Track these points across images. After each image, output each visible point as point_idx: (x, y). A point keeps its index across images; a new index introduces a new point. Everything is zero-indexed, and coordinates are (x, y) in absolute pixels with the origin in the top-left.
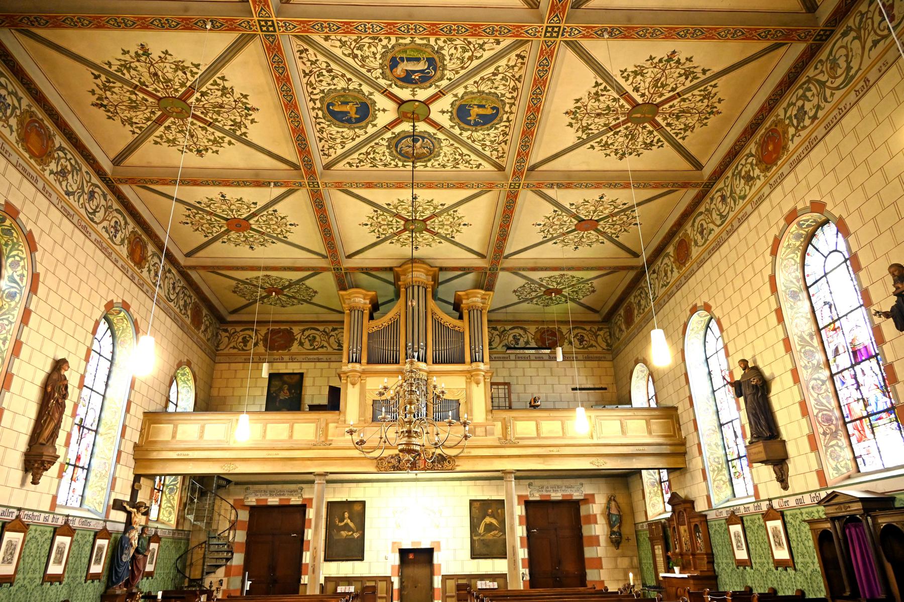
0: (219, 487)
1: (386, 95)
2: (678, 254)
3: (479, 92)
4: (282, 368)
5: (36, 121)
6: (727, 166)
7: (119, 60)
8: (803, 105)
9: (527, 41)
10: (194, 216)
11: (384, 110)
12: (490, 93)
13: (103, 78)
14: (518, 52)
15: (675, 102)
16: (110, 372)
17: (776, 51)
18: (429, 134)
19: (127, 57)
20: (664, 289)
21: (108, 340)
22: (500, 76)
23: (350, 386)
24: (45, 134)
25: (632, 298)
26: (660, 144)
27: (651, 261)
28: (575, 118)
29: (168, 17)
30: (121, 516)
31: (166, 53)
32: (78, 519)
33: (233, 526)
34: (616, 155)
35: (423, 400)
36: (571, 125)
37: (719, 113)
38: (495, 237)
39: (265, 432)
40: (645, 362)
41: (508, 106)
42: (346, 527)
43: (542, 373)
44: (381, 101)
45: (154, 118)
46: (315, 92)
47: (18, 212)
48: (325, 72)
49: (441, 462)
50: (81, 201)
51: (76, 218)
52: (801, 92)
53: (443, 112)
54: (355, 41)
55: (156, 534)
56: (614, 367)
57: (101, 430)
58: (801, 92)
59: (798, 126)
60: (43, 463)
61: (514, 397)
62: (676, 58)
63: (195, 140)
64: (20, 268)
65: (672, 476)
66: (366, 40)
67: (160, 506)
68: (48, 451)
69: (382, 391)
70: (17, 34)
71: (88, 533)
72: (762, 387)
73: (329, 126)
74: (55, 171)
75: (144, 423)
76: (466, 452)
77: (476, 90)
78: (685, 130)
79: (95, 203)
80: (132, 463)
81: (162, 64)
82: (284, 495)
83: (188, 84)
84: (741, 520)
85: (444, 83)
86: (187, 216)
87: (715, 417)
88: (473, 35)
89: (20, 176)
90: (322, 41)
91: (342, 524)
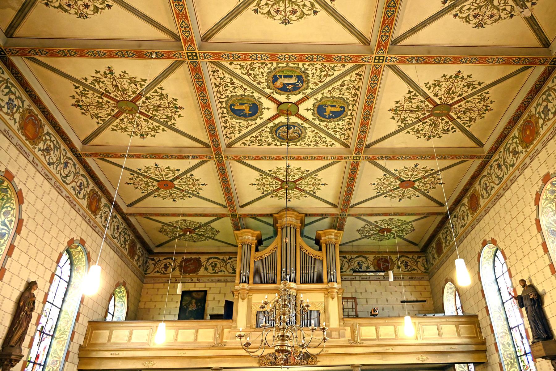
1: (270, 99)
2: (471, 204)
3: (331, 97)
4: (191, 287)
5: (33, 116)
6: (500, 144)
7: (93, 77)
8: (547, 105)
9: (363, 65)
10: (136, 179)
11: (268, 109)
12: (339, 97)
13: (81, 88)
14: (357, 72)
15: (462, 103)
16: (67, 291)
17: (525, 71)
18: (298, 124)
19: (98, 75)
20: (463, 229)
21: (68, 267)
22: (345, 87)
23: (240, 300)
24: (37, 124)
25: (441, 235)
26: (454, 130)
27: (452, 209)
28: (396, 114)
29: (127, 50)
31: (125, 72)
34: (424, 137)
36: (393, 118)
37: (491, 110)
38: (344, 193)
39: (177, 336)
40: (452, 281)
41: (351, 106)
43: (379, 289)
44: (266, 103)
45: (113, 114)
46: (222, 97)
47: (13, 177)
48: (229, 85)
50: (58, 169)
51: (53, 180)
52: (544, 97)
53: (307, 110)
54: (250, 65)
56: (430, 285)
57: (56, 335)
58: (544, 97)
59: (545, 118)
60: (11, 361)
61: (359, 308)
62: (461, 76)
63: (140, 128)
64: (10, 216)
66: (257, 64)
68: (15, 352)
69: (264, 305)
70: (26, 60)
72: (538, 300)
73: (231, 119)
74: (42, 148)
75: (88, 329)
76: (325, 351)
77: (329, 96)
78: (470, 121)
79: (68, 170)
80: (77, 361)
81: (121, 80)
83: (138, 92)
85: (308, 91)
86: (130, 179)
87: (505, 323)
88: (327, 61)
89: (18, 152)
90: (227, 65)
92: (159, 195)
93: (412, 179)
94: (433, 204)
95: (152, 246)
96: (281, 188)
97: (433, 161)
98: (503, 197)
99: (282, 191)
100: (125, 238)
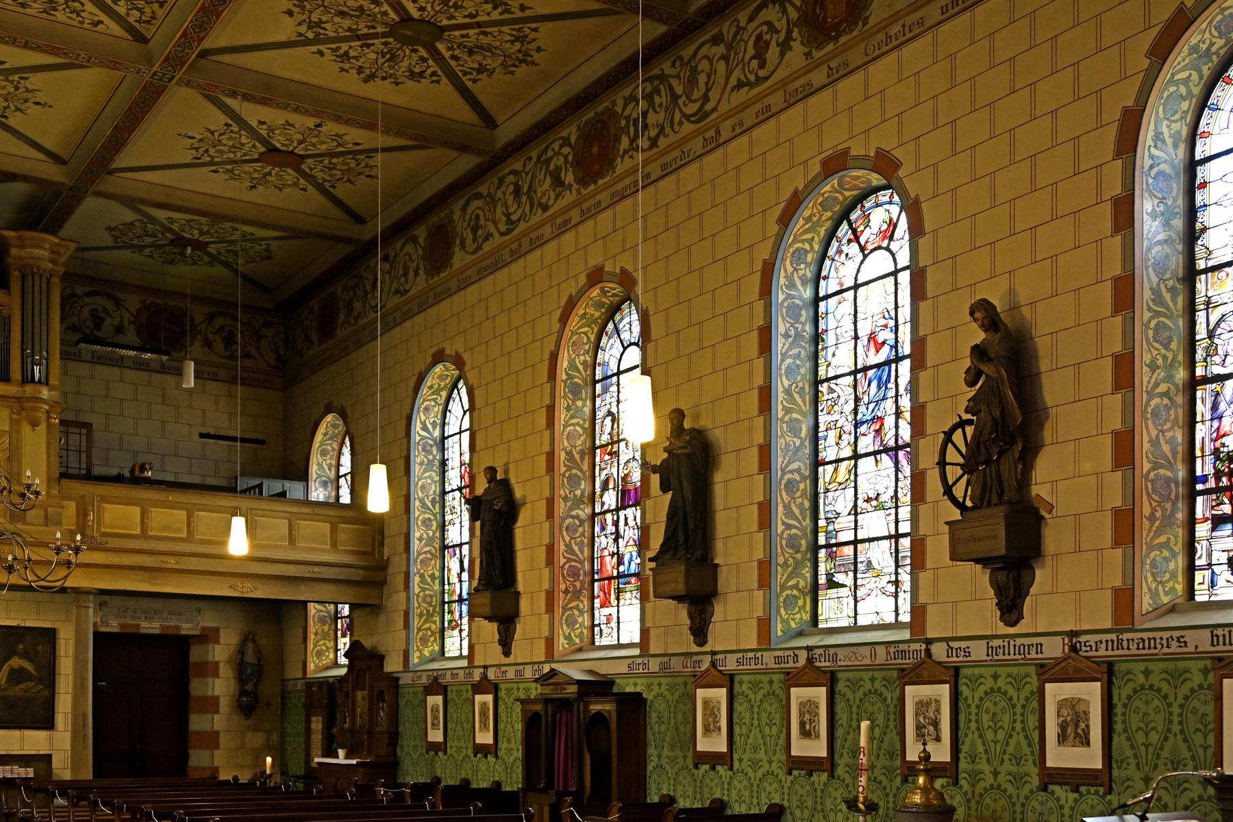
98: (505, 270)
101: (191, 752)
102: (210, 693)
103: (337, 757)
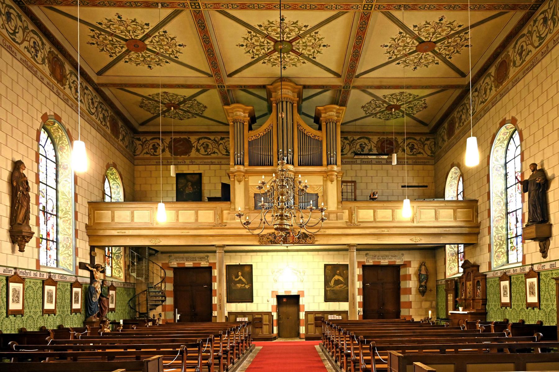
0: (150, 255)
20: (482, 105)
25: (456, 113)
27: (475, 80)
30: (87, 274)
32: (57, 275)
33: (164, 280)
35: (291, 192)
42: (240, 281)
49: (304, 239)
55: (112, 285)
65: (467, 249)
67: (112, 267)
71: (66, 284)
82: (195, 260)
84: (510, 278)
91: (237, 279)
92: (130, 59)
93: (434, 40)
94: (453, 73)
95: (135, 125)
96: (275, 51)
97: (463, 13)
99: (276, 55)
100: (104, 115)
101: (402, 310)
102: (408, 287)
103: (459, 310)
